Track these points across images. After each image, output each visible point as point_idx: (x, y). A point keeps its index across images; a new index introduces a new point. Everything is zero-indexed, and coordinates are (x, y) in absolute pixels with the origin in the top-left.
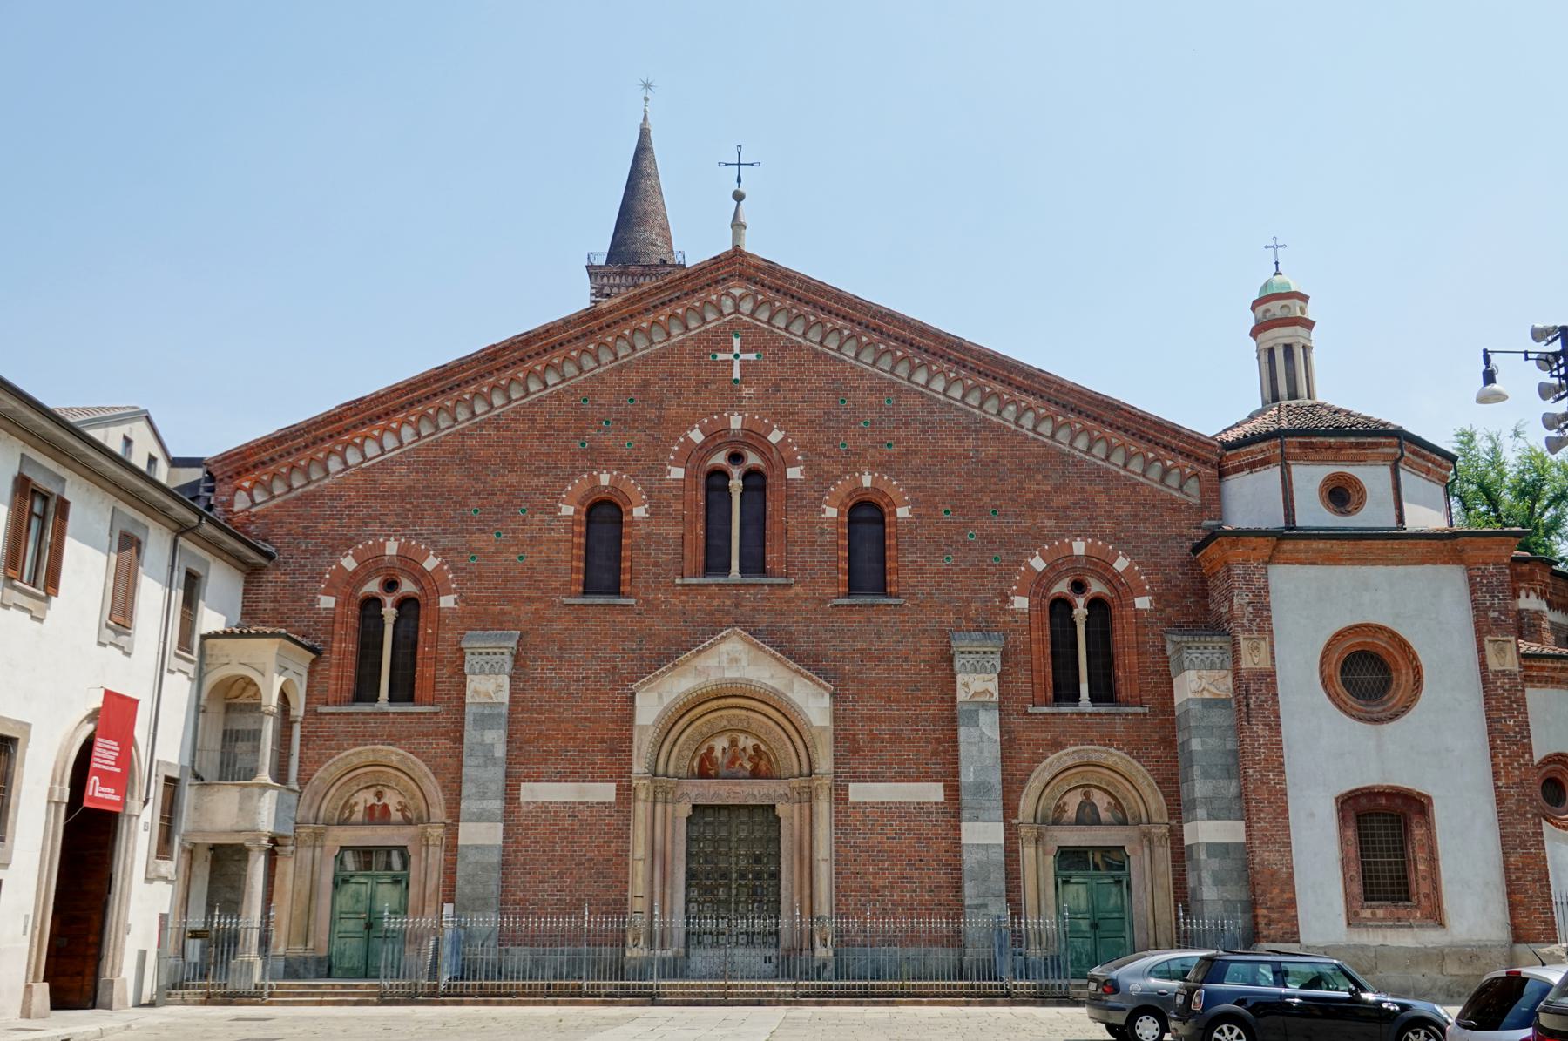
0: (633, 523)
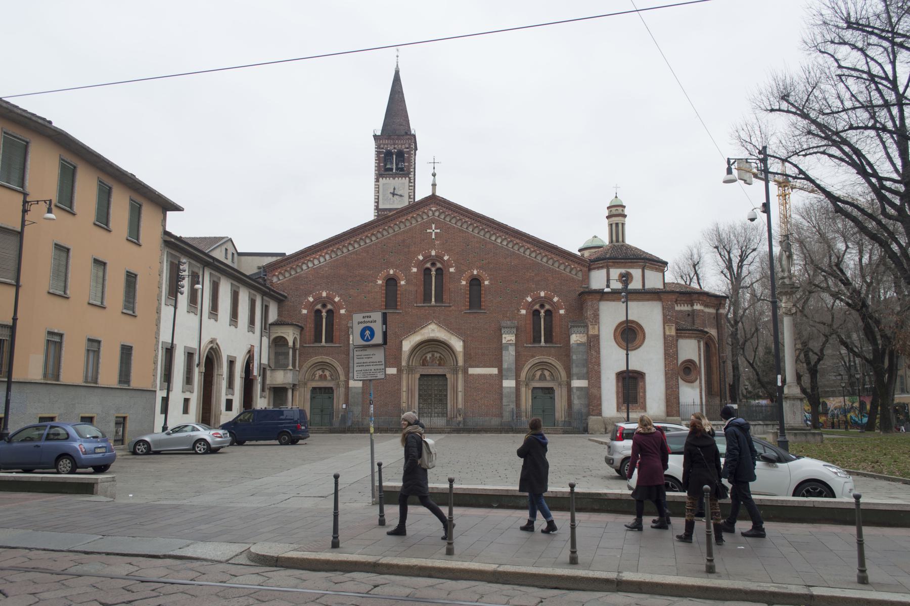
0: (401, 286)
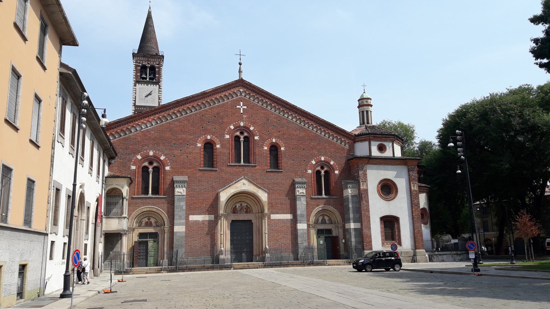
0: (216, 149)
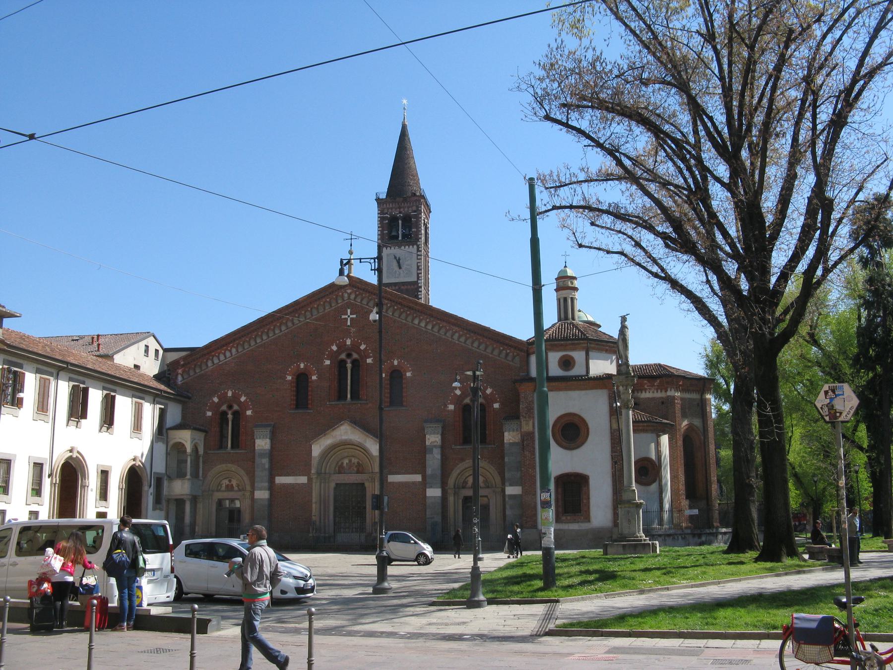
0: (313, 381)
